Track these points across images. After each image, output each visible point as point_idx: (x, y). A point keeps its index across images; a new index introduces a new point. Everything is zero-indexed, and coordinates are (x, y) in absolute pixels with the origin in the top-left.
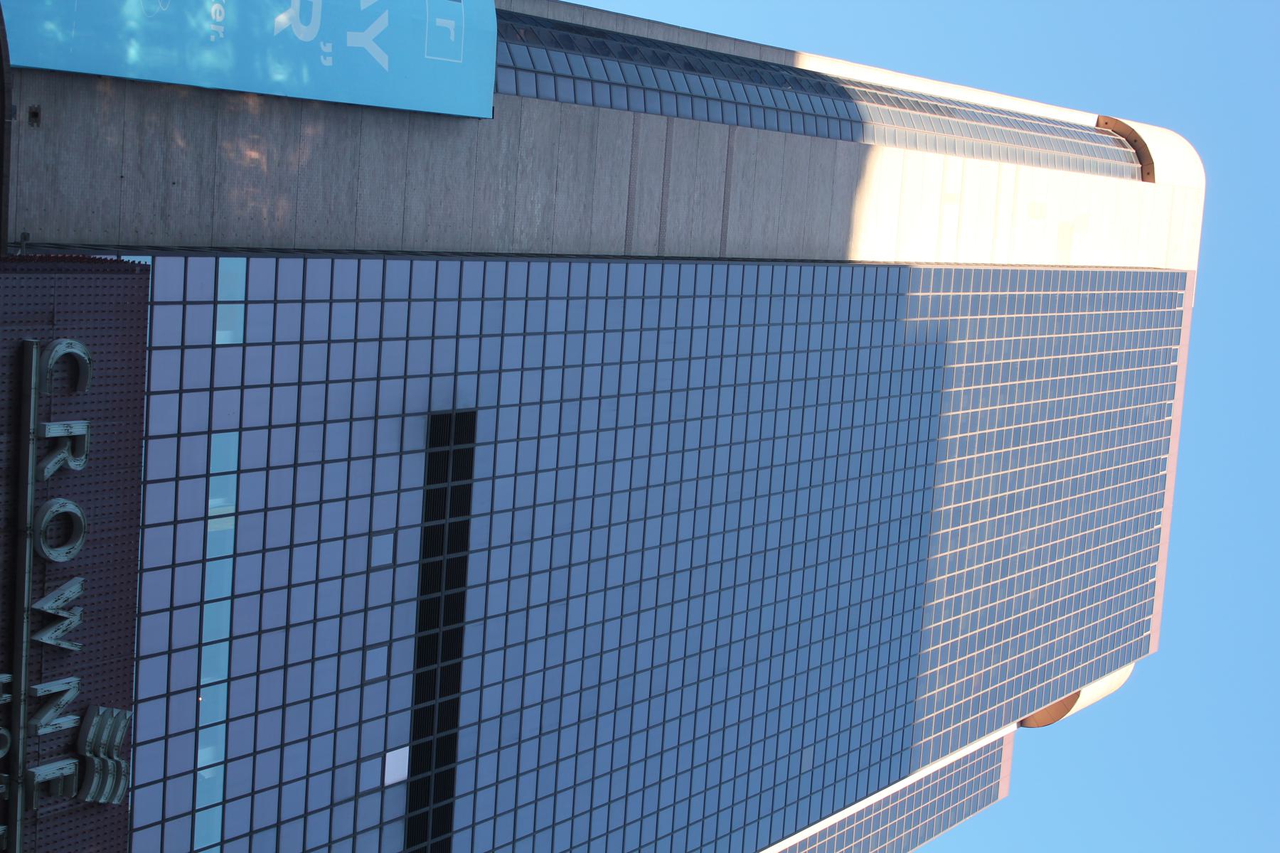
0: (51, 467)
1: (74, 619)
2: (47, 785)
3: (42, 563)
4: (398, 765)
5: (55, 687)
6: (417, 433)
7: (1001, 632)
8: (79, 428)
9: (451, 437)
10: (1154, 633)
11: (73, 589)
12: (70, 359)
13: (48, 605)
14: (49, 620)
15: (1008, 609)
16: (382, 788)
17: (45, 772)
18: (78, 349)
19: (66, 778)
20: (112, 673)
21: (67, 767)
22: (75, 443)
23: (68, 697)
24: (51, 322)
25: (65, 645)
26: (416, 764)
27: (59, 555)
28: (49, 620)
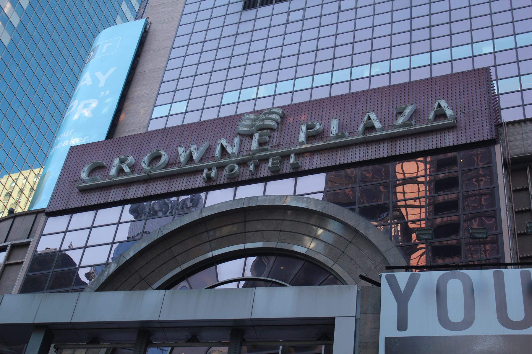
0: (127, 170)
2: (260, 144)
3: (168, 165)
5: (218, 148)
6: (251, 14)
8: (116, 162)
11: (181, 150)
12: (91, 172)
13: (182, 159)
14: (190, 159)
17: (254, 145)
18: (86, 168)
19: (260, 136)
20: (226, 125)
21: (256, 136)
22: (122, 161)
23: (224, 143)
24: (75, 181)
25: (202, 148)
27: (164, 158)
28: (190, 159)
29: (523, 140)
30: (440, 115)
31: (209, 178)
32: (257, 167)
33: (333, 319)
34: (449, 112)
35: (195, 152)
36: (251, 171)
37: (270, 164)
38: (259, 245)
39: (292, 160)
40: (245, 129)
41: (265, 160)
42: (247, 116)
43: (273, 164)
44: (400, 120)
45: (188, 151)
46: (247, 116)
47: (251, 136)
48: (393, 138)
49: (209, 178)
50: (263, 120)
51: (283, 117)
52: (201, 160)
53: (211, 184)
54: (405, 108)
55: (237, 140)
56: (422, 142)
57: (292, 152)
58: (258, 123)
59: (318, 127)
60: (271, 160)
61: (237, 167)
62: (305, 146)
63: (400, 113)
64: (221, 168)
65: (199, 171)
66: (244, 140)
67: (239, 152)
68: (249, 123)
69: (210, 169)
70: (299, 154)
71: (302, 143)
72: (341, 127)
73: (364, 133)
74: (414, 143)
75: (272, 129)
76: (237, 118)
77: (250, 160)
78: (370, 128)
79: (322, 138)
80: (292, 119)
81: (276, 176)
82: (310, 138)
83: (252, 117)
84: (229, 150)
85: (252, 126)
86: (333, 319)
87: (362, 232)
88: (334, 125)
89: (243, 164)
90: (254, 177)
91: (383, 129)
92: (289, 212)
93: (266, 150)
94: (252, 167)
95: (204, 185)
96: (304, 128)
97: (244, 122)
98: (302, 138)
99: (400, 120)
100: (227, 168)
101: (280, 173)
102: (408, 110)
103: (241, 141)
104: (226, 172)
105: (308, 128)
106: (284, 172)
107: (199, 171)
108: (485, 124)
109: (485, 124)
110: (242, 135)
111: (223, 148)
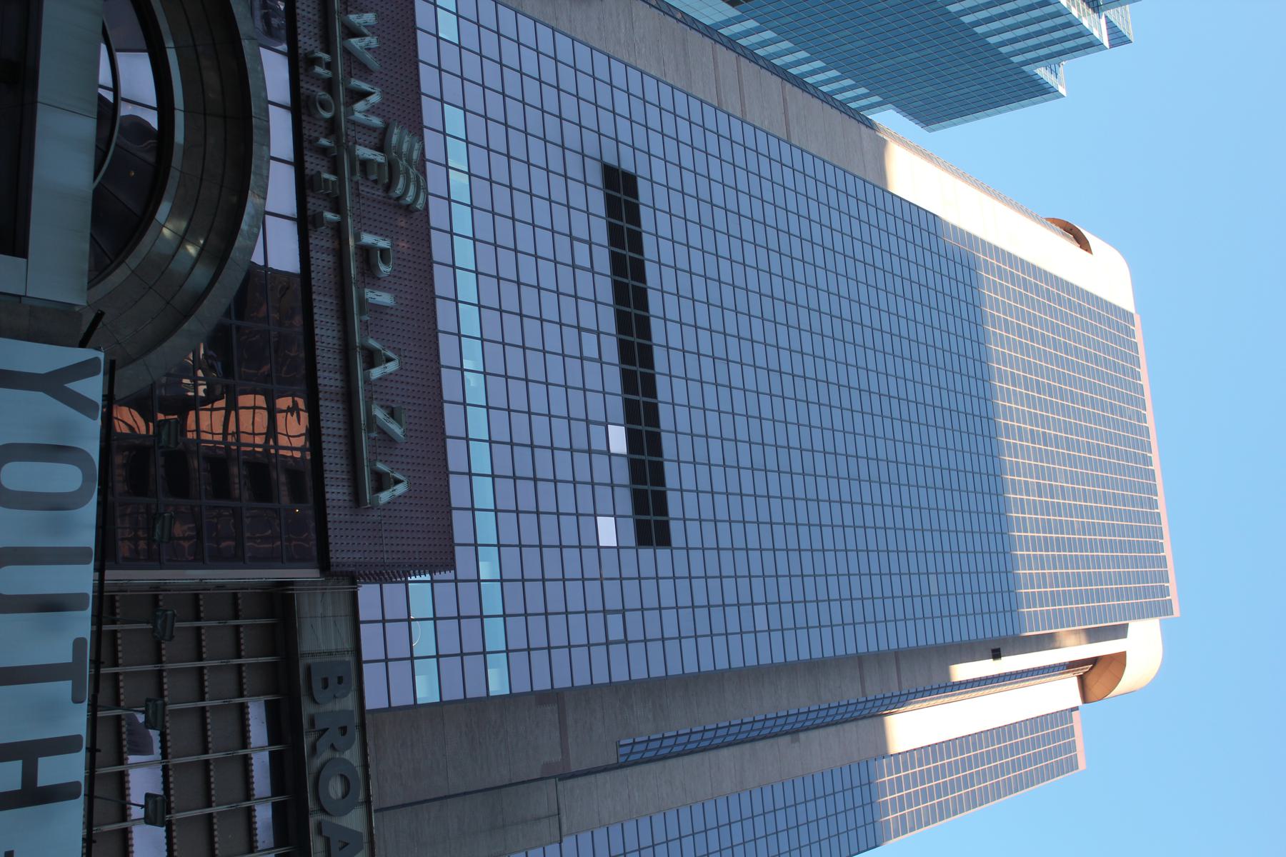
1: (373, 41)
2: (365, 163)
4: (618, 439)
5: (365, 86)
6: (595, 177)
7: (1059, 544)
9: (620, 189)
10: (1173, 596)
11: (369, 18)
13: (353, 17)
14: (352, 32)
15: (1060, 527)
16: (608, 453)
17: (364, 152)
19: (380, 164)
20: (407, 106)
21: (380, 158)
23: (374, 99)
26: (632, 438)
28: (352, 32)
29: (323, 617)
30: (381, 482)
31: (314, 61)
32: (324, 151)
33: (24, 254)
34: (385, 497)
35: (363, 44)
36: (317, 139)
37: (326, 176)
38: (179, 137)
39: (329, 216)
40: (394, 139)
41: (335, 168)
42: (417, 146)
43: (326, 180)
44: (379, 413)
45: (365, 31)
46: (417, 146)
47: (380, 148)
48: (349, 397)
49: (314, 61)
50: (407, 172)
51: (409, 210)
52: (348, 53)
53: (301, 64)
54: (400, 423)
55: (376, 121)
56: (336, 446)
57: (344, 218)
58: (402, 164)
59: (384, 269)
60: (333, 178)
61: (327, 115)
62: (351, 242)
63: (392, 414)
64: (330, 85)
65: (328, 46)
66: (375, 134)
67: (354, 123)
68: (405, 147)
69: (328, 66)
70: (339, 231)
71: (357, 238)
72: (379, 309)
73: (363, 348)
74: (337, 432)
75: (389, 187)
76: (417, 128)
77: (338, 141)
78: (372, 359)
79: (363, 274)
80: (403, 224)
81: (304, 185)
82: (366, 253)
83: (415, 155)
84: (360, 106)
85: (399, 153)
86: (24, 254)
87: (186, 326)
88: (384, 298)
89: (332, 127)
90: (306, 144)
91: (367, 381)
92: (234, 199)
93: (352, 172)
94: (324, 142)
95: (300, 51)
96: (384, 244)
97: (407, 139)
98: (368, 239)
99: (379, 413)
100: (327, 97)
101: (308, 192)
102: (396, 429)
103: (374, 129)
104: (322, 94)
105: (383, 251)
106: (309, 199)
107: (328, 46)
108: (357, 555)
109: (357, 555)
110: (384, 133)
111: (364, 95)
